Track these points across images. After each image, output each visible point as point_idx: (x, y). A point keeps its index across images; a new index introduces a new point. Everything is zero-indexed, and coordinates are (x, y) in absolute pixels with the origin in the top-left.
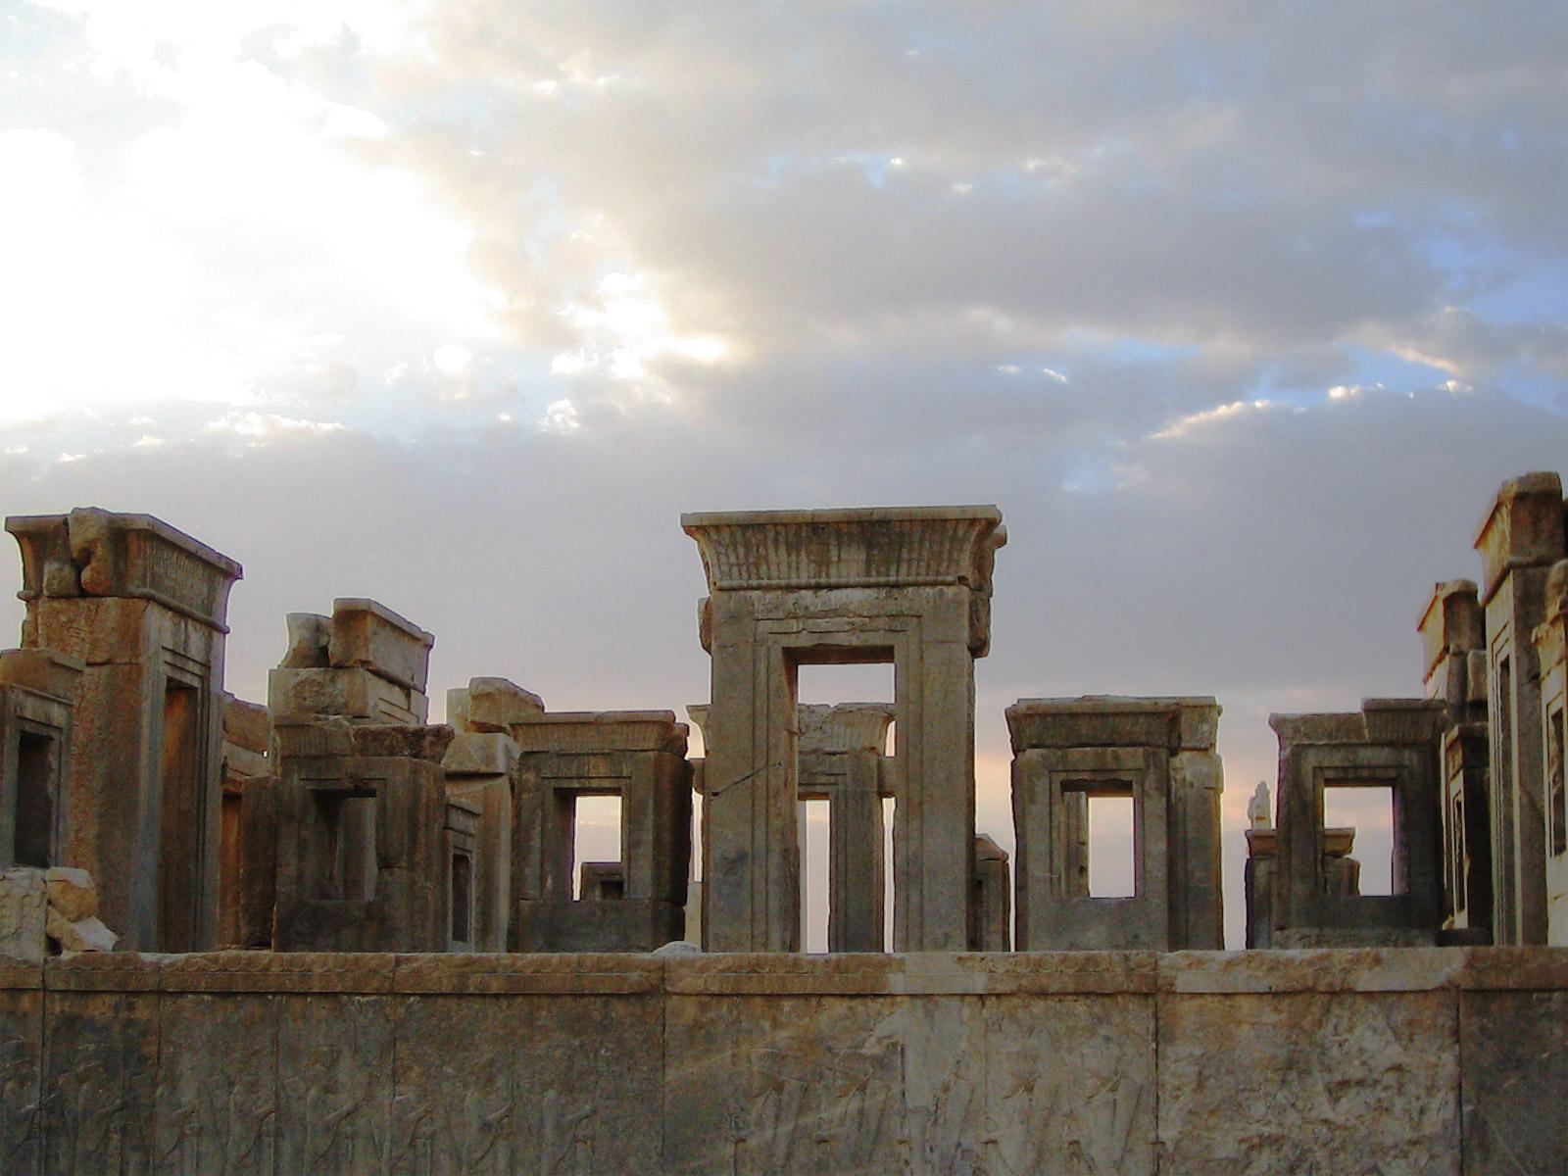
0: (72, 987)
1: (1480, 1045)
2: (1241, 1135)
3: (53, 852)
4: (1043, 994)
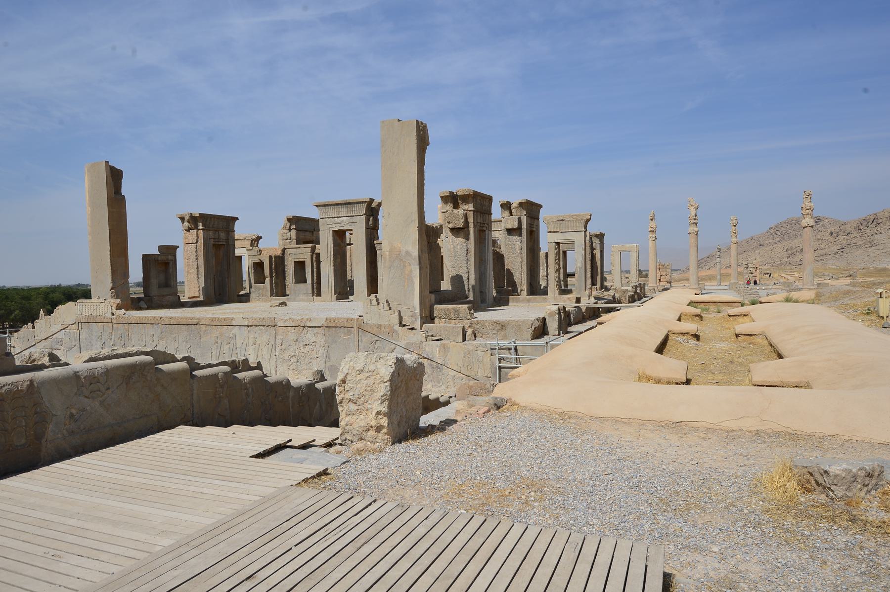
3: (172, 284)
4: (256, 326)
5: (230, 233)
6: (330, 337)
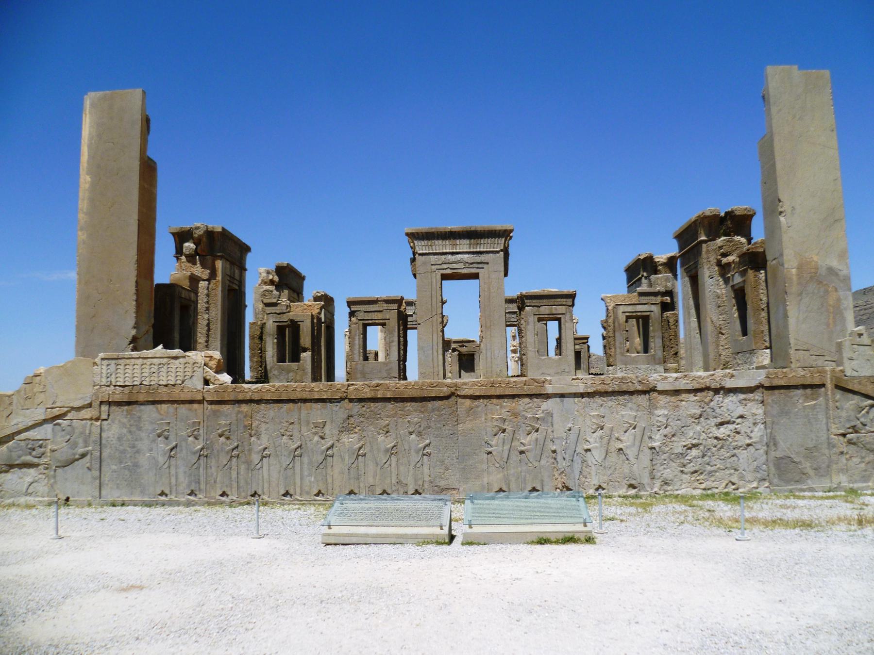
0: (215, 399)
1: (772, 407)
2: (684, 444)
5: (243, 271)
6: (775, 406)
